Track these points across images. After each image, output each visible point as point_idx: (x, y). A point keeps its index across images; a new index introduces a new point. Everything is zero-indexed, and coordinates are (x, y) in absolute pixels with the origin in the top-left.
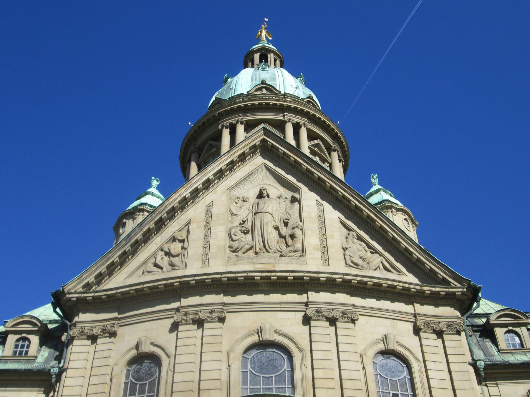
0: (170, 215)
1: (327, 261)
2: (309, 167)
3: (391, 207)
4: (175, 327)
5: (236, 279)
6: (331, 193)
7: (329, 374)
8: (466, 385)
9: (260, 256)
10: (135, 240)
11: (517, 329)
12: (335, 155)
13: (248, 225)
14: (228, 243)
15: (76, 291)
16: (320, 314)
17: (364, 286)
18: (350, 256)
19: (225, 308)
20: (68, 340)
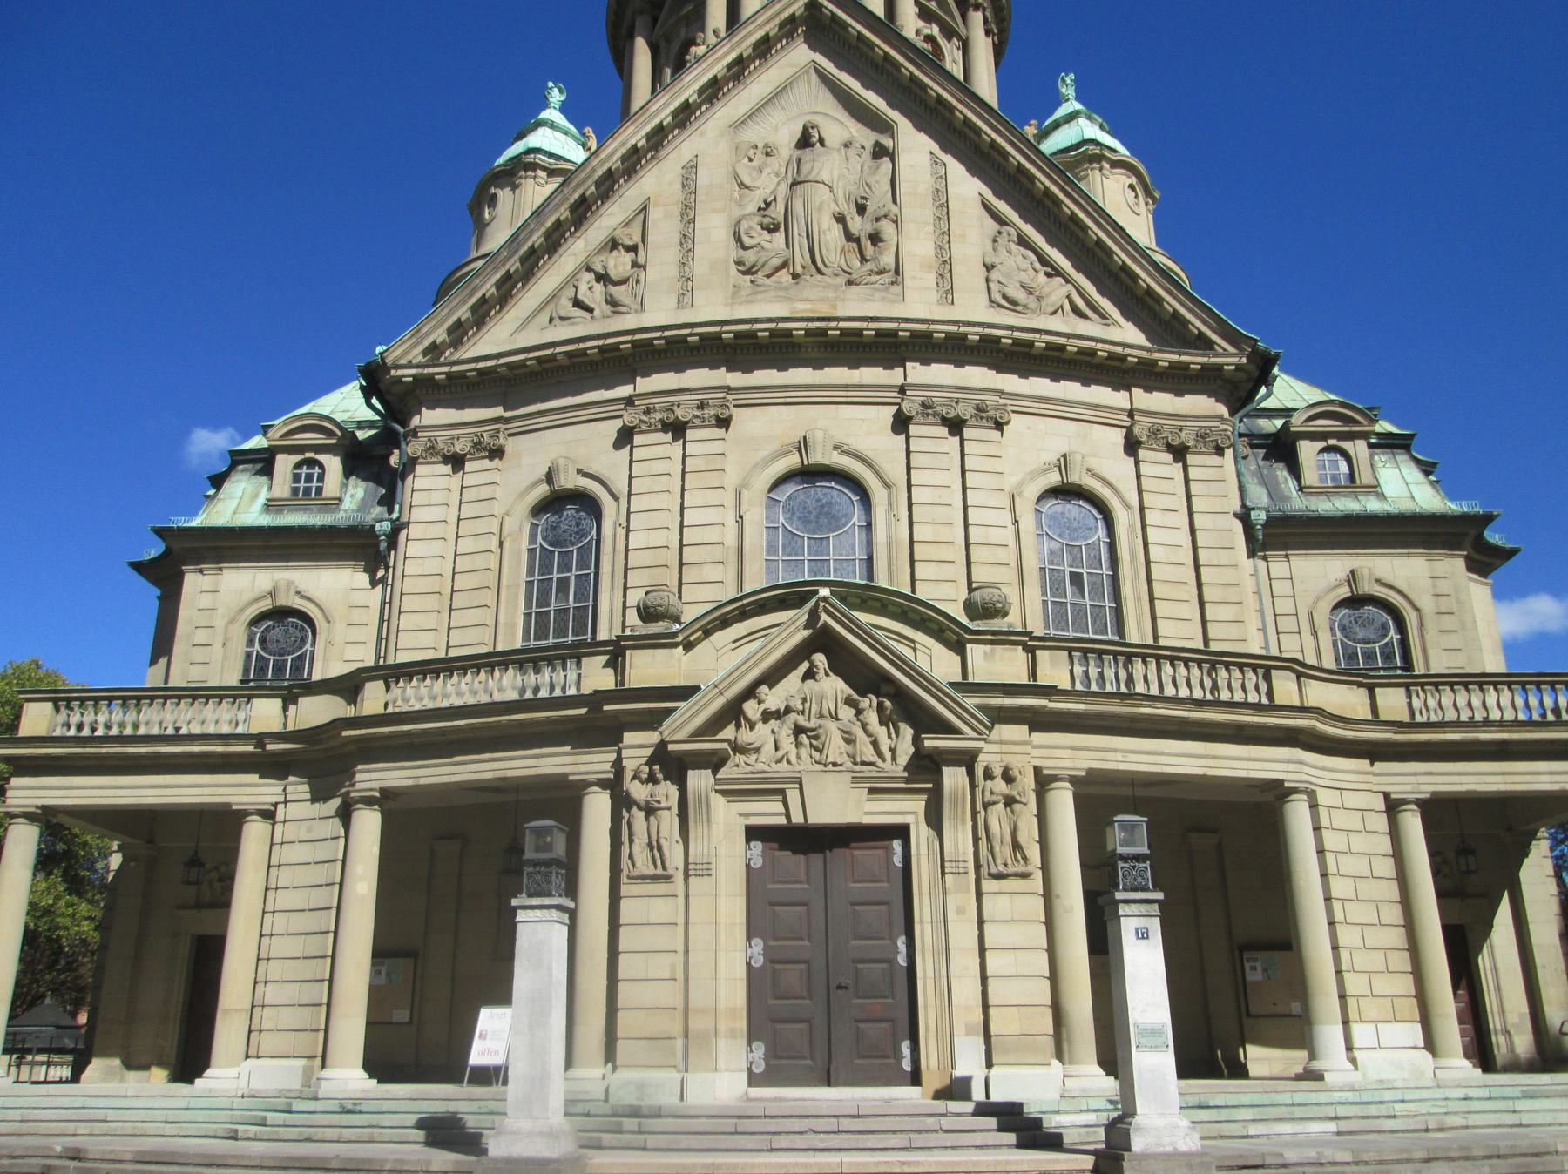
0: (603, 188)
1: (948, 295)
2: (916, 72)
3: (1099, 158)
4: (625, 438)
5: (752, 335)
6: (966, 137)
7: (944, 534)
8: (1223, 557)
9: (803, 282)
10: (529, 248)
11: (1347, 445)
12: (977, 18)
13: (778, 211)
14: (734, 252)
15: (410, 362)
16: (930, 411)
17: (1027, 350)
18: (999, 282)
19: (729, 397)
20: (404, 464)
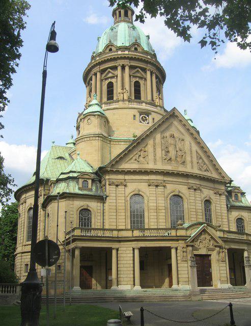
1: (192, 167)
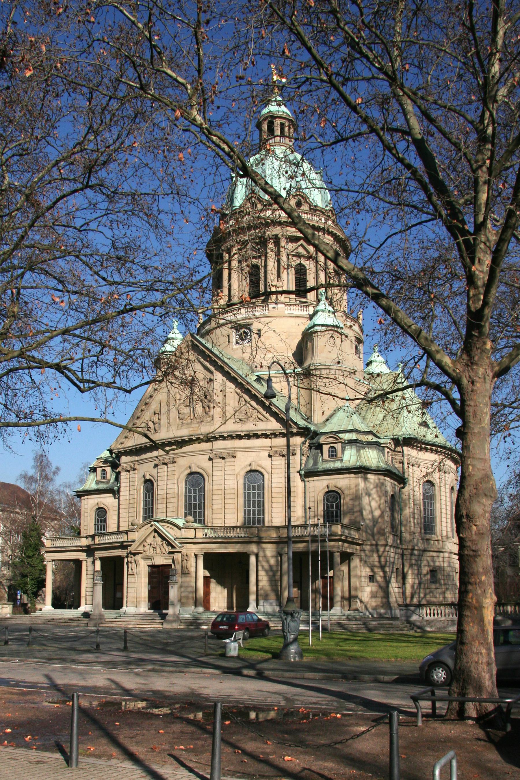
11: (335, 445)
